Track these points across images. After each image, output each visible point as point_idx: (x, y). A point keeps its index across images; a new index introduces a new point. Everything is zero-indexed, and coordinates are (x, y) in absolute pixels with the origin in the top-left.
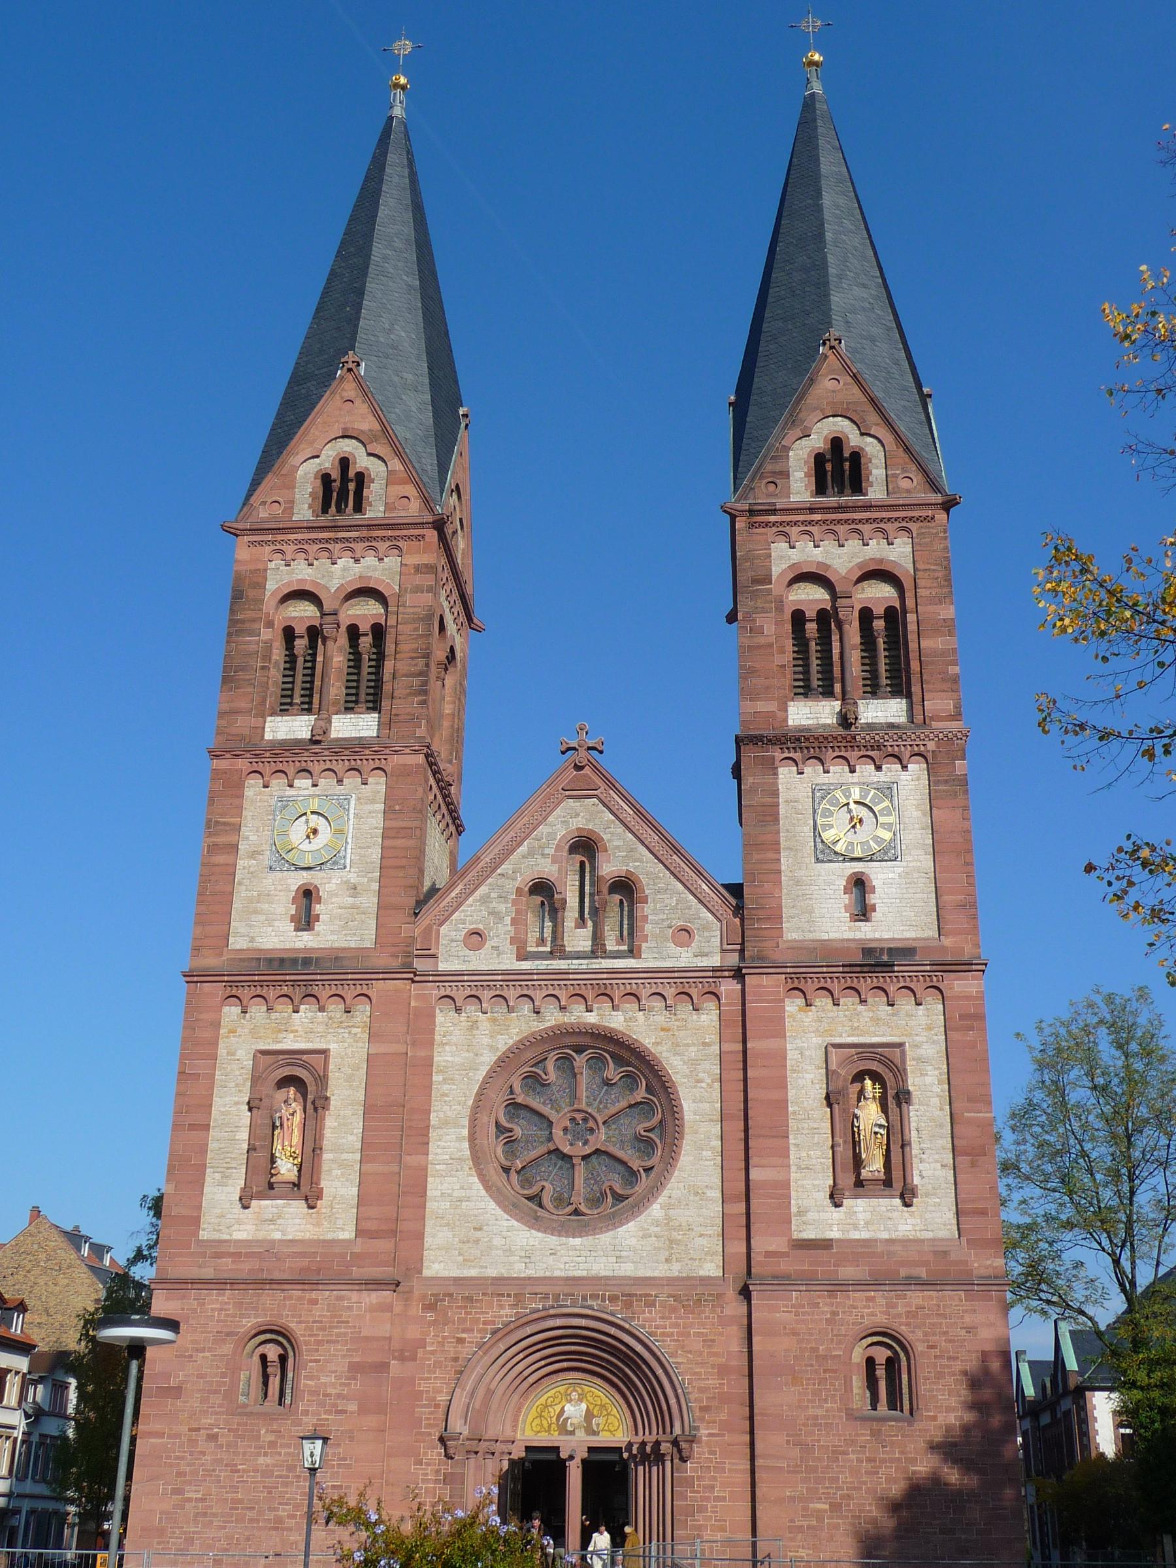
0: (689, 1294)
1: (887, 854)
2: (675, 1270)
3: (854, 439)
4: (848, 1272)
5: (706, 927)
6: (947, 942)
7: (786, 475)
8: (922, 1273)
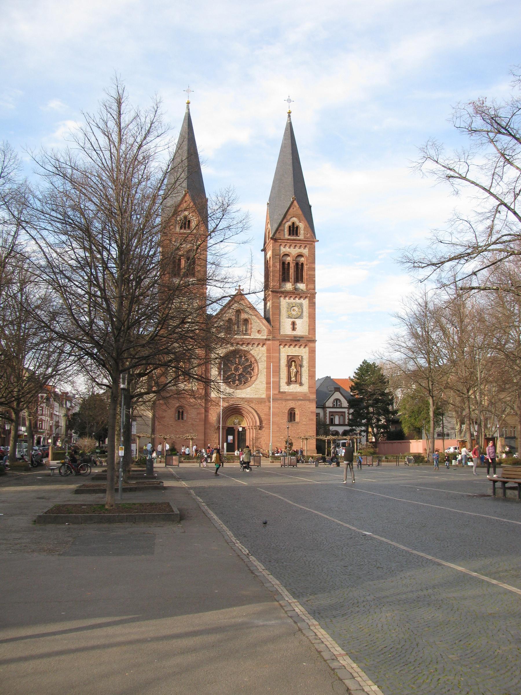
0: (260, 401)
1: (300, 317)
2: (256, 396)
3: (297, 223)
4: (288, 398)
5: (264, 330)
6: (310, 336)
7: (284, 230)
8: (302, 398)
